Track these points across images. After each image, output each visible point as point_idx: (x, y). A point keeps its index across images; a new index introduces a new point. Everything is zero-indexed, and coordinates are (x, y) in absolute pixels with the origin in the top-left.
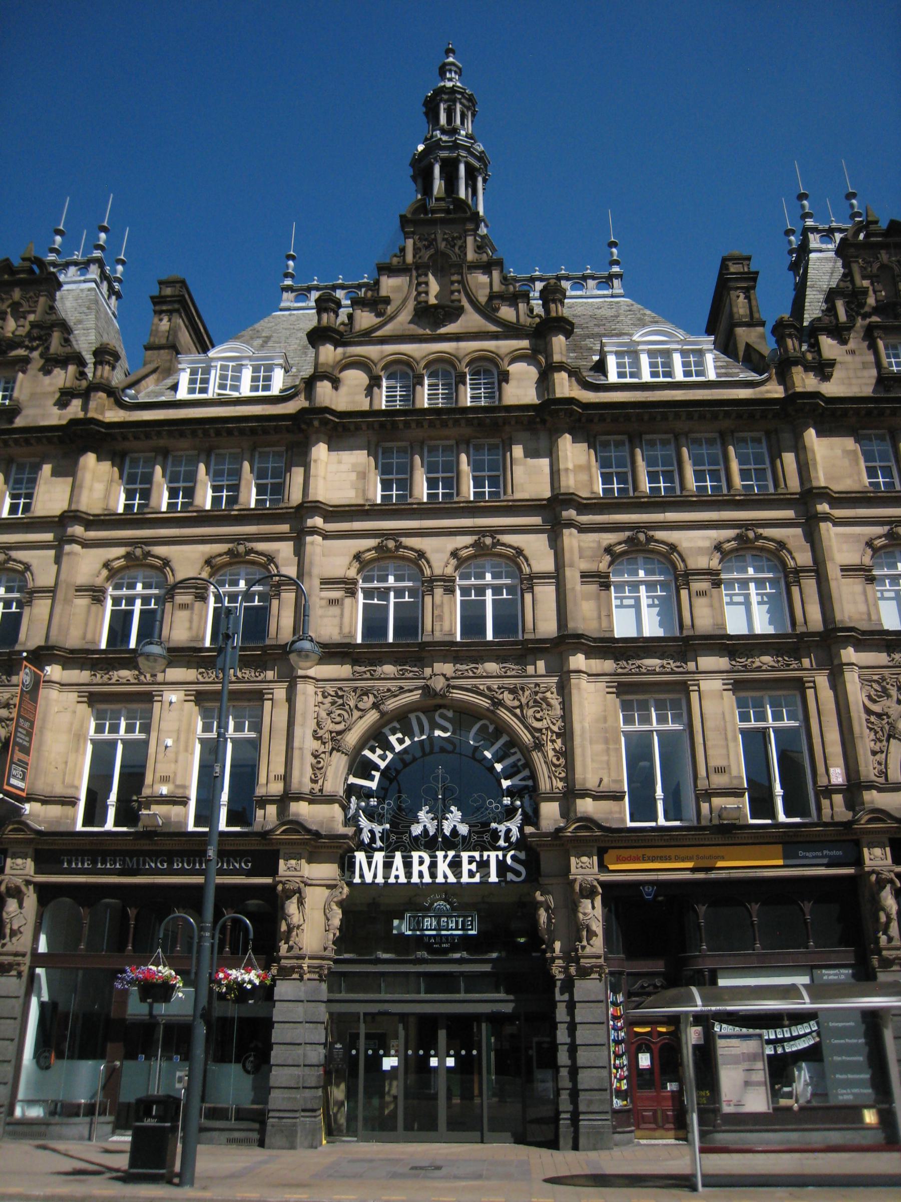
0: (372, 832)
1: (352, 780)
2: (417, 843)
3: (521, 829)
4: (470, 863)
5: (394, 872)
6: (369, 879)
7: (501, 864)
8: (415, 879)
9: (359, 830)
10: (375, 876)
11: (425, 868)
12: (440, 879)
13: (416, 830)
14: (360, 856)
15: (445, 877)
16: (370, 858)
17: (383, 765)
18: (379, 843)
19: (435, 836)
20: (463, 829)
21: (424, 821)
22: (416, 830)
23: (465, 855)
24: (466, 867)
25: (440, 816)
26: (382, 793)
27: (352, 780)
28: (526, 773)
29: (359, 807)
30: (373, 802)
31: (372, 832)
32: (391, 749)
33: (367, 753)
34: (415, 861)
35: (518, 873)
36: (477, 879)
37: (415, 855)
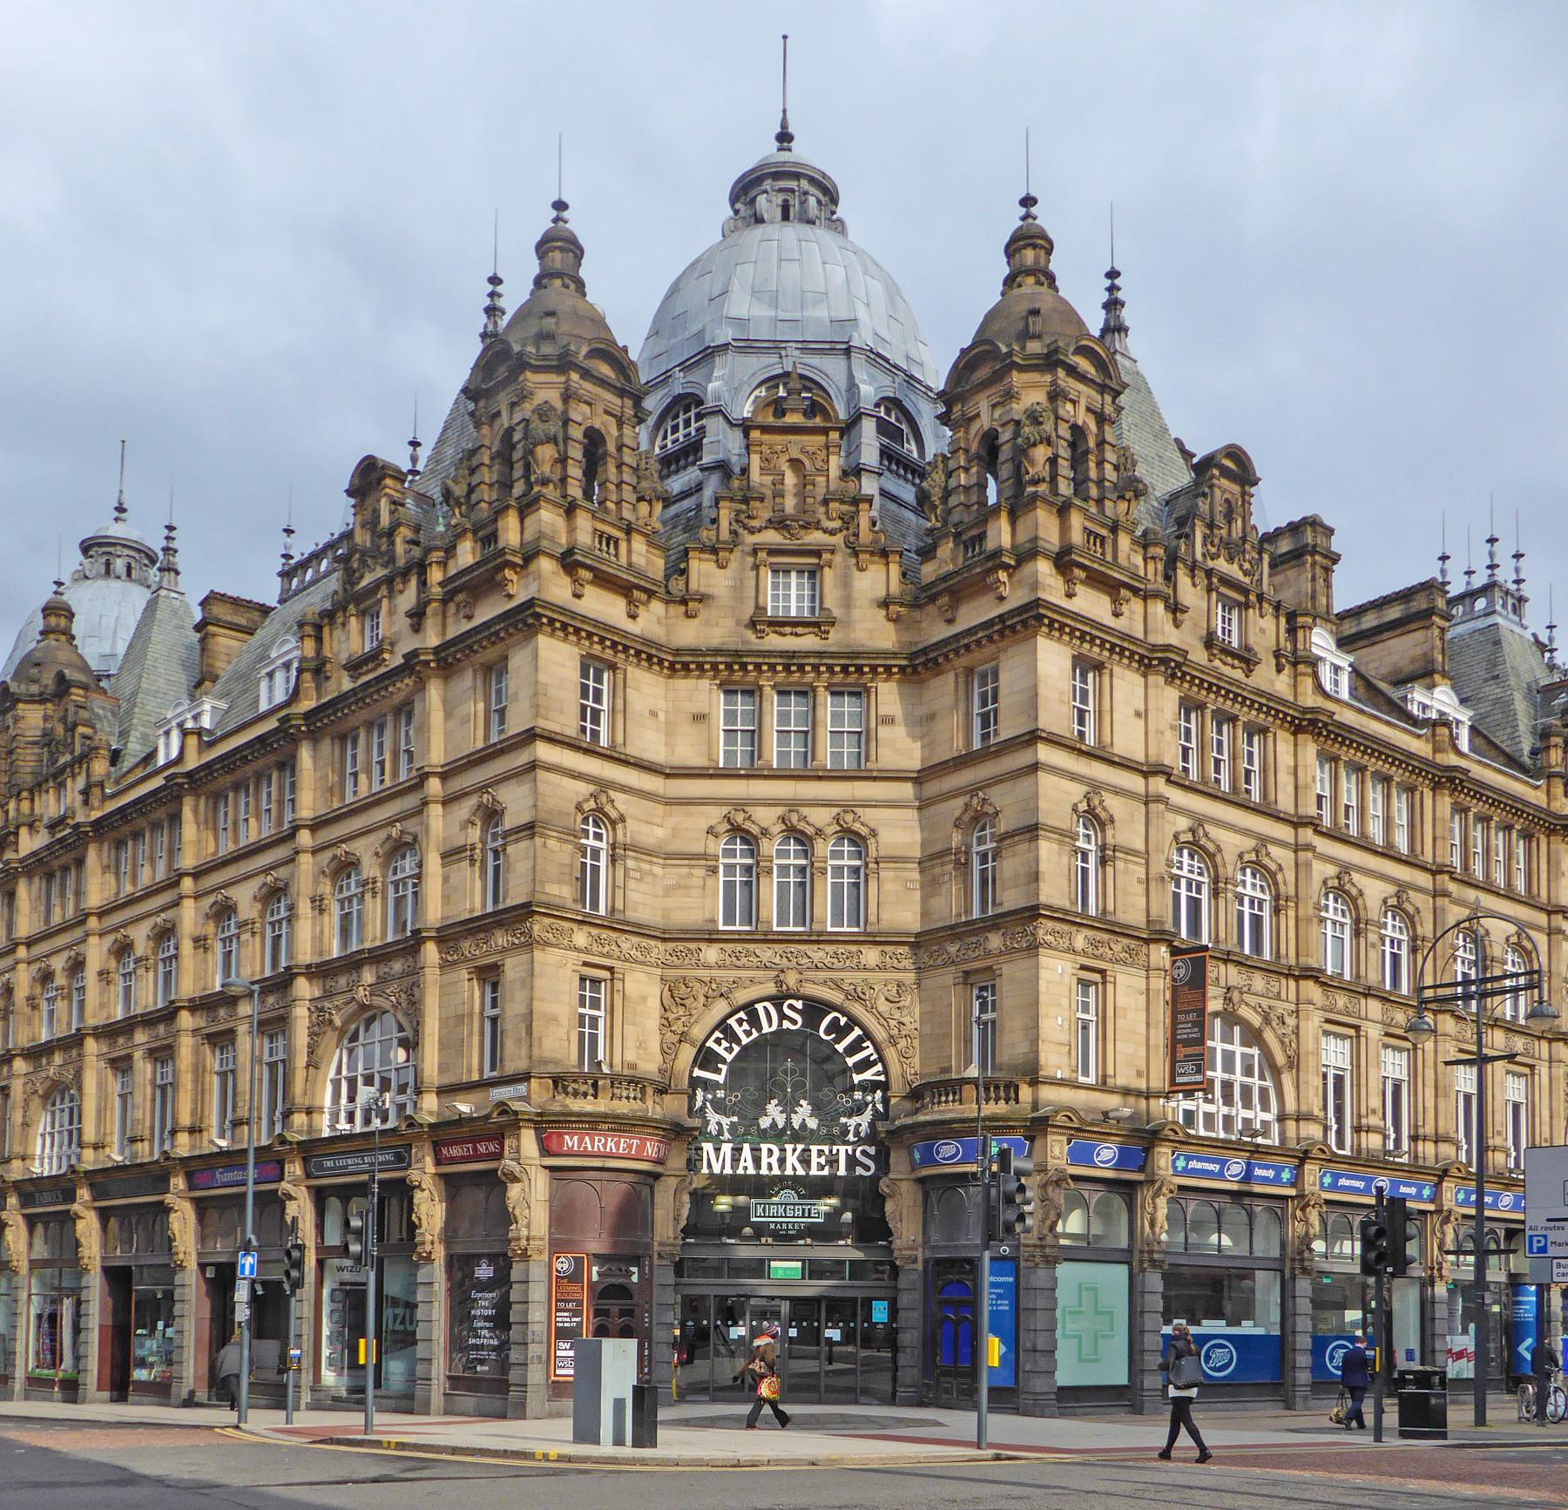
0: (719, 1124)
1: (697, 1072)
2: (764, 1135)
3: (872, 1125)
4: (819, 1156)
5: (742, 1164)
6: (717, 1170)
7: (852, 1161)
8: (764, 1171)
9: (707, 1123)
10: (723, 1167)
11: (774, 1161)
12: (789, 1172)
13: (765, 1123)
14: (708, 1147)
15: (794, 1169)
16: (717, 1150)
17: (729, 1057)
18: (727, 1136)
19: (784, 1129)
20: (813, 1123)
21: (774, 1114)
22: (765, 1123)
23: (814, 1149)
24: (814, 1160)
25: (789, 1107)
26: (729, 1086)
27: (697, 1072)
28: (879, 1067)
29: (705, 1100)
30: (720, 1094)
31: (719, 1124)
32: (738, 1041)
33: (710, 1044)
34: (764, 1153)
35: (867, 1168)
36: (826, 1172)
37: (764, 1147)
